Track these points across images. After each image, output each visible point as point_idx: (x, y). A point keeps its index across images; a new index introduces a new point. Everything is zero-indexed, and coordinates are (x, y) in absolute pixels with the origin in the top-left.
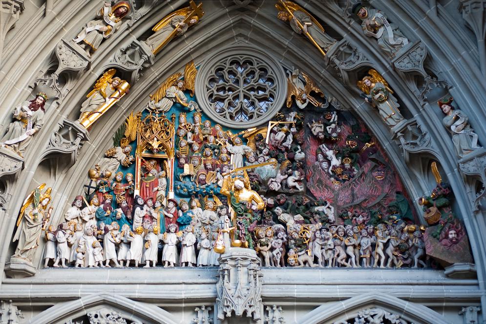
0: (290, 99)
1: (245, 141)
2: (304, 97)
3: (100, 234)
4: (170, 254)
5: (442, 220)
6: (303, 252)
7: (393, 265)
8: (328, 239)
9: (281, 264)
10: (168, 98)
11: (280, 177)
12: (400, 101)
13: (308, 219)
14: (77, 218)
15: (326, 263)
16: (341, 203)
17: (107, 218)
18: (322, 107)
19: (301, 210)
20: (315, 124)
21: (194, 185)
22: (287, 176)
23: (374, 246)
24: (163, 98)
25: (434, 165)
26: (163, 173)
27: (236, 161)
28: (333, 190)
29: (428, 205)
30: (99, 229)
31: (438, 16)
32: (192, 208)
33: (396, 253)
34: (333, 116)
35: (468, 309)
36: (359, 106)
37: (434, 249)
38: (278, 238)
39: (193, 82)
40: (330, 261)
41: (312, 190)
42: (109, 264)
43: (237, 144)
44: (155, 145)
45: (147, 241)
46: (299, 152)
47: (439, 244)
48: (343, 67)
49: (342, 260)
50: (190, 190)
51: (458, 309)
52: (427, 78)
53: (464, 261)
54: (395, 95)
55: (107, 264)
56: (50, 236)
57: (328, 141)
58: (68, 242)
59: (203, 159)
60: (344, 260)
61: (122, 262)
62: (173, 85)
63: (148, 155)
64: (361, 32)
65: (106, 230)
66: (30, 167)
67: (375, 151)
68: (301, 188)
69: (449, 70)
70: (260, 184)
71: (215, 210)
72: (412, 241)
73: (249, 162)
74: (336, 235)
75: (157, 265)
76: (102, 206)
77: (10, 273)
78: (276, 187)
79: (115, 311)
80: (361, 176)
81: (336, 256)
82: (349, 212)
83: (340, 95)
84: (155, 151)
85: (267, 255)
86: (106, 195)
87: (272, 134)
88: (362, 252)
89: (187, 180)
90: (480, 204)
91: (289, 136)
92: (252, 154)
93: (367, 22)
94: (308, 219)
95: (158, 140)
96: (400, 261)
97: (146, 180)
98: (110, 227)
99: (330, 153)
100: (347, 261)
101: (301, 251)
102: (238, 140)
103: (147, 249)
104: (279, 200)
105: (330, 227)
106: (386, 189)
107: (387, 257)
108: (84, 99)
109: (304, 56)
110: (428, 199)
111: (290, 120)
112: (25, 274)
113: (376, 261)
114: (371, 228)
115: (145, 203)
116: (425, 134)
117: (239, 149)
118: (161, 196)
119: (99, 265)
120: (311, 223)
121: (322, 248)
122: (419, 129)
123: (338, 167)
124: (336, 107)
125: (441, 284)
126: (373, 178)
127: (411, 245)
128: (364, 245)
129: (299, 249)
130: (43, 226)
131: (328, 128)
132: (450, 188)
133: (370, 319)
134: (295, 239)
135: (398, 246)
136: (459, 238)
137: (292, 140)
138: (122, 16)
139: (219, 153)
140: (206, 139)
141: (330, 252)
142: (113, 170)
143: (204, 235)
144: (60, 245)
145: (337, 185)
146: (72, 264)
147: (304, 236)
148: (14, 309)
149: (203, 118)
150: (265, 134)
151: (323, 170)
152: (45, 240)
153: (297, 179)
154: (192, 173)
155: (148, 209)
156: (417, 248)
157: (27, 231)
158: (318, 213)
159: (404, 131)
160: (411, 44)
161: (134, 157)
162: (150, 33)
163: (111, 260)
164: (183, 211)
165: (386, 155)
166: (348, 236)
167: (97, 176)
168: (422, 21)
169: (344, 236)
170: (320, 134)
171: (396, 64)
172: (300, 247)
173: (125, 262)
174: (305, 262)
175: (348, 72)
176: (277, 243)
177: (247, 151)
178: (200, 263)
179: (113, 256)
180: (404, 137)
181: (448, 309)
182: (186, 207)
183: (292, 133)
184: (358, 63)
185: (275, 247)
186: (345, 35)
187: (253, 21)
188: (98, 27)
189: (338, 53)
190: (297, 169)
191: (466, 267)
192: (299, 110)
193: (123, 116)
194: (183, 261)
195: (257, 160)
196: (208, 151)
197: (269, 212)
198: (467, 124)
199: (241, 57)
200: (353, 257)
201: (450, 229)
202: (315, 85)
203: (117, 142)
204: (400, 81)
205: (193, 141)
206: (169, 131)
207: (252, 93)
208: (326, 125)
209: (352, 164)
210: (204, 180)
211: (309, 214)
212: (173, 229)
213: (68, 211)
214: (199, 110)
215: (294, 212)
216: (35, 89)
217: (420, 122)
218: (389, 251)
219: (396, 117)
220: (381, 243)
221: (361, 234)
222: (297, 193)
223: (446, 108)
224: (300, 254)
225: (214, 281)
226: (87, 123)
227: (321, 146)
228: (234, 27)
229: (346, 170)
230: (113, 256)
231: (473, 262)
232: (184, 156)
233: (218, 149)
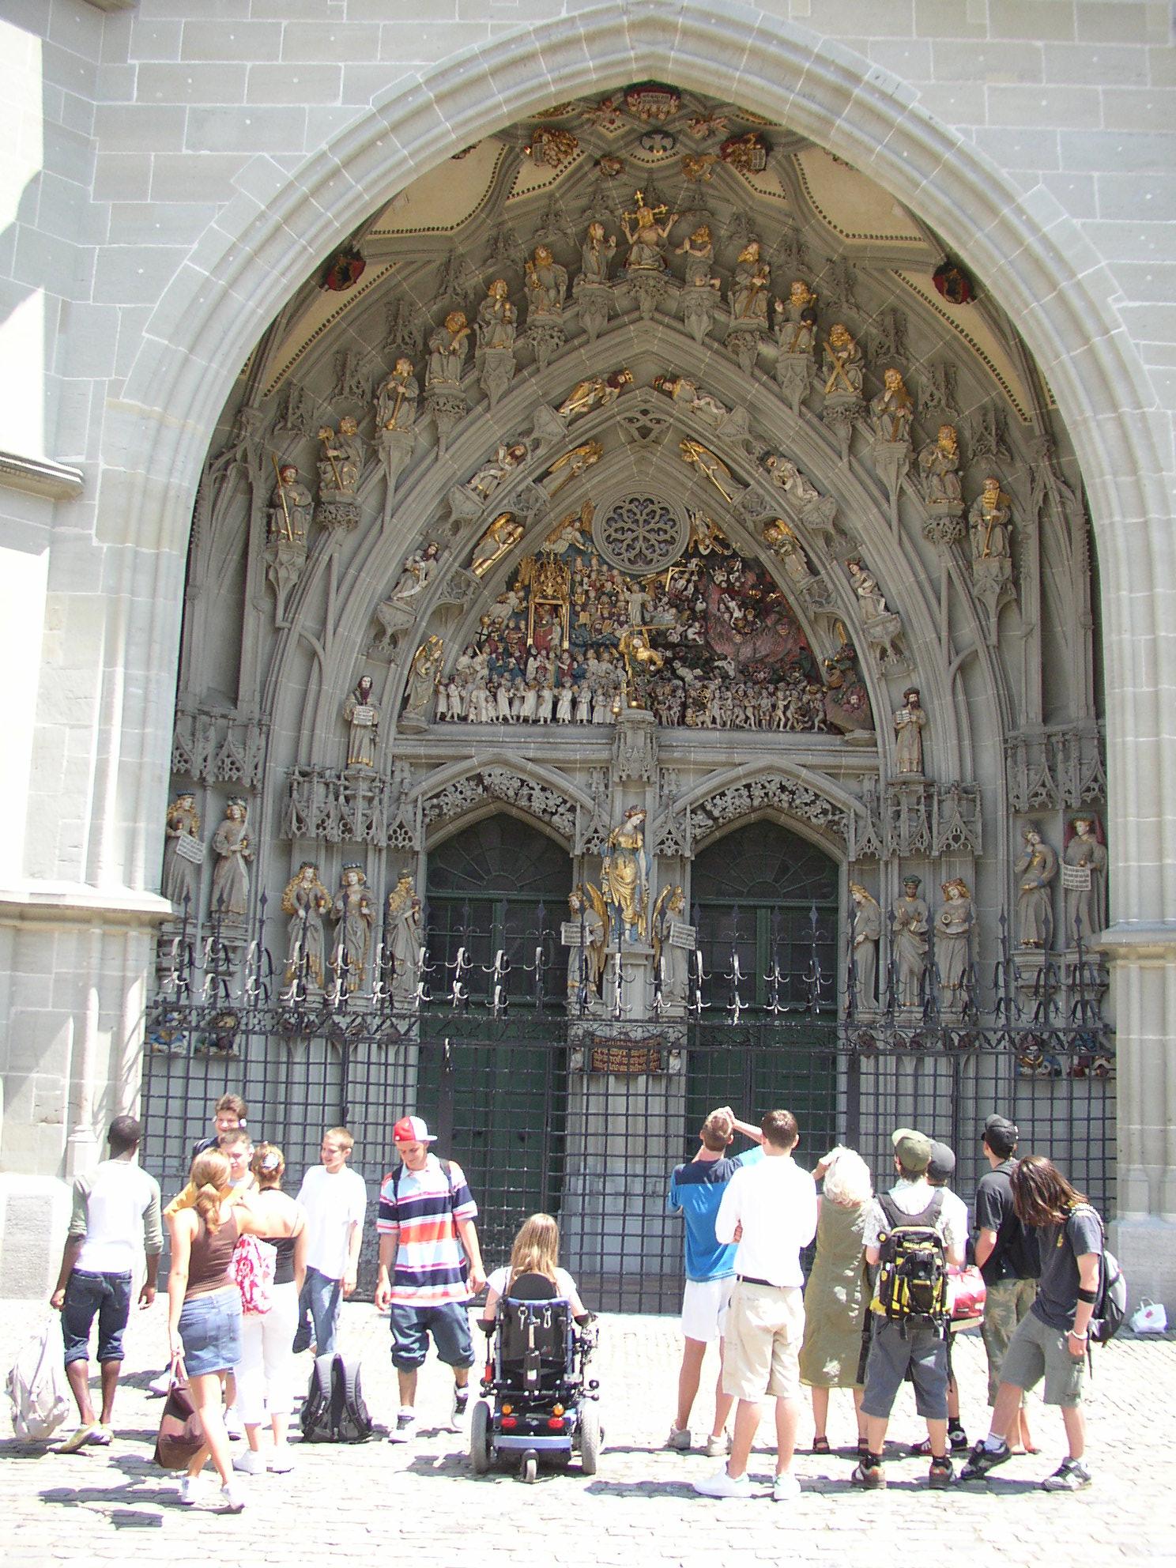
4: (564, 711)
7: (793, 728)
12: (807, 555)
15: (724, 724)
23: (774, 707)
25: (839, 624)
29: (831, 668)
37: (837, 717)
52: (837, 537)
54: (802, 548)
56: (442, 688)
65: (500, 685)
66: (422, 618)
85: (664, 714)
98: (503, 682)
107: (787, 719)
108: (477, 545)
114: (771, 688)
138: (519, 459)
143: (600, 691)
146: (464, 719)
152: (436, 692)
162: (547, 473)
178: (595, 721)
179: (507, 712)
188: (492, 472)
212: (568, 685)
215: (692, 667)
216: (426, 536)
217: (826, 579)
218: (789, 714)
220: (781, 704)
223: (855, 568)
226: (479, 572)
230: (507, 712)
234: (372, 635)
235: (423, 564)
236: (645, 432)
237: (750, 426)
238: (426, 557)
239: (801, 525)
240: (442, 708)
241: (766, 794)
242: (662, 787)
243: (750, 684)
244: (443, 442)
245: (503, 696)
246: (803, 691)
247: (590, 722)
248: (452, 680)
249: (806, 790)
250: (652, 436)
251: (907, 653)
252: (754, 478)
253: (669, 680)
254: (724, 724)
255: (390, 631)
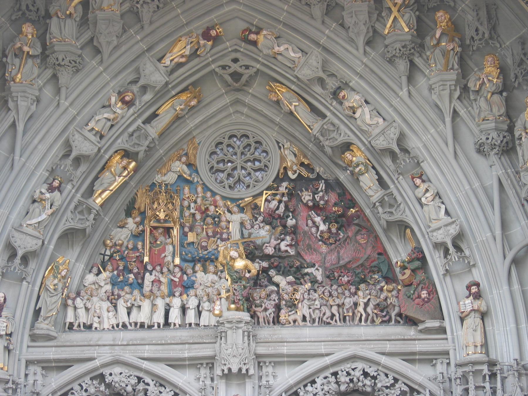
0: (282, 171)
1: (242, 210)
2: (295, 168)
3: (114, 299)
4: (175, 316)
5: (415, 281)
6: (293, 312)
8: (315, 300)
9: (274, 322)
10: (173, 172)
11: (274, 242)
13: (299, 279)
14: (94, 283)
16: (328, 265)
17: (120, 284)
18: (311, 177)
19: (292, 272)
20: (305, 193)
21: (197, 251)
22: (280, 241)
23: (356, 304)
24: (168, 172)
25: (408, 231)
26: (169, 240)
27: (234, 229)
28: (321, 253)
29: (403, 268)
30: (113, 294)
31: (409, 97)
32: (195, 272)
33: (376, 312)
34: (321, 185)
35: (439, 361)
36: (343, 177)
38: (270, 300)
39: (195, 157)
40: (317, 320)
41: (302, 253)
42: (122, 326)
43: (235, 213)
44: (162, 216)
45: (155, 305)
46: (291, 219)
47: (413, 303)
48: (327, 143)
49: (327, 318)
50: (194, 256)
51: (431, 360)
53: (434, 318)
54: (373, 167)
55: (120, 327)
56: (70, 302)
57: (316, 207)
58: (85, 307)
59: (205, 227)
60: (329, 319)
61: (133, 324)
62: (177, 160)
63: (156, 224)
64: (342, 111)
65: (119, 296)
67: (358, 217)
68: (292, 252)
69: (420, 145)
70: (256, 249)
71: (216, 273)
72: (390, 300)
73: (246, 229)
74: (322, 295)
75: (164, 325)
76: (115, 273)
77: (34, 338)
78: (270, 251)
79: (127, 369)
80: (346, 240)
81: (321, 315)
82: (335, 273)
83: (326, 166)
84: (162, 221)
85: (261, 315)
86: (119, 262)
87: (266, 203)
88: (345, 311)
89: (192, 246)
90: (447, 268)
91: (282, 204)
92: (249, 221)
93: (347, 104)
94: (299, 279)
95: (164, 211)
96: (379, 318)
97: (155, 247)
98: (122, 293)
99: (318, 219)
100: (332, 319)
101: (291, 311)
102: (235, 209)
103: (155, 312)
104: (273, 263)
105: (318, 287)
106: (369, 250)
107: (368, 315)
109: (293, 132)
110: (403, 262)
111: (282, 189)
112: (49, 338)
113: (358, 318)
114: (353, 289)
115: (154, 269)
116: (400, 204)
117: (237, 217)
118: (168, 261)
119: (113, 327)
120: (301, 284)
121: (310, 308)
122: (395, 199)
123: (325, 232)
124: (324, 176)
125: (415, 340)
126: (357, 242)
127: (389, 303)
128: (347, 304)
129: (290, 309)
130: (63, 294)
131: (316, 196)
132: (422, 252)
133: (352, 372)
134: (286, 301)
135: (378, 305)
136: (431, 297)
137: (284, 209)
139: (220, 221)
140: (207, 209)
141: (317, 311)
142: (125, 239)
143: (205, 298)
144: (79, 311)
145: (324, 249)
146: (89, 327)
147: (294, 297)
148: (39, 370)
149: (205, 189)
150: (260, 202)
151: (312, 234)
152: (65, 306)
153: (288, 243)
154: (195, 240)
155: (157, 274)
156: (394, 306)
157: (48, 300)
158: (307, 274)
159: (382, 202)
160: (386, 123)
161: (144, 226)
163: (123, 323)
164: (187, 275)
165: (368, 220)
166: (333, 297)
167: (111, 244)
168: (395, 102)
169: (330, 296)
170: (309, 202)
171: (373, 143)
172: (291, 307)
173: (136, 324)
174: (295, 321)
175: (332, 148)
176: (270, 305)
177: (244, 219)
178: (202, 323)
179: (125, 319)
180: (381, 206)
181: (420, 361)
182: (190, 271)
183: (284, 202)
184: (341, 139)
185: (268, 307)
186: (328, 114)
187: (247, 100)
189: (323, 132)
190: (289, 234)
191: (435, 324)
192: (291, 180)
193: (132, 190)
194: (187, 322)
195: (252, 227)
196: (209, 220)
197: (264, 274)
198: (436, 195)
199: (239, 132)
200: (337, 315)
201: (422, 288)
202: (305, 156)
203: (129, 213)
204: (376, 155)
205: (196, 210)
206: (174, 202)
207: (249, 164)
208: (314, 194)
209: (338, 229)
210: (206, 247)
211: (300, 276)
212: (177, 294)
213: (86, 278)
214: (201, 182)
215: (285, 274)
218: (369, 310)
219: (374, 188)
221: (344, 295)
222: (290, 256)
223: (418, 181)
224: (290, 313)
225: (214, 341)
227: (310, 213)
228: (231, 105)
229: (333, 234)
230: (125, 319)
231: (444, 320)
232: (188, 225)
233: (218, 217)
234: (6, 258)
235: (48, 195)
236: (236, 76)
237: (323, 67)
238: (51, 189)
239: (371, 149)
240: (70, 318)
241: (351, 381)
242: (260, 378)
243: (335, 287)
244: (63, 91)
245: (122, 306)
246: (381, 289)
247: (198, 325)
248: (78, 294)
249: (387, 375)
250: (244, 79)
251: (467, 252)
252: (330, 111)
253: (266, 286)
254: (314, 321)
255: (20, 253)
